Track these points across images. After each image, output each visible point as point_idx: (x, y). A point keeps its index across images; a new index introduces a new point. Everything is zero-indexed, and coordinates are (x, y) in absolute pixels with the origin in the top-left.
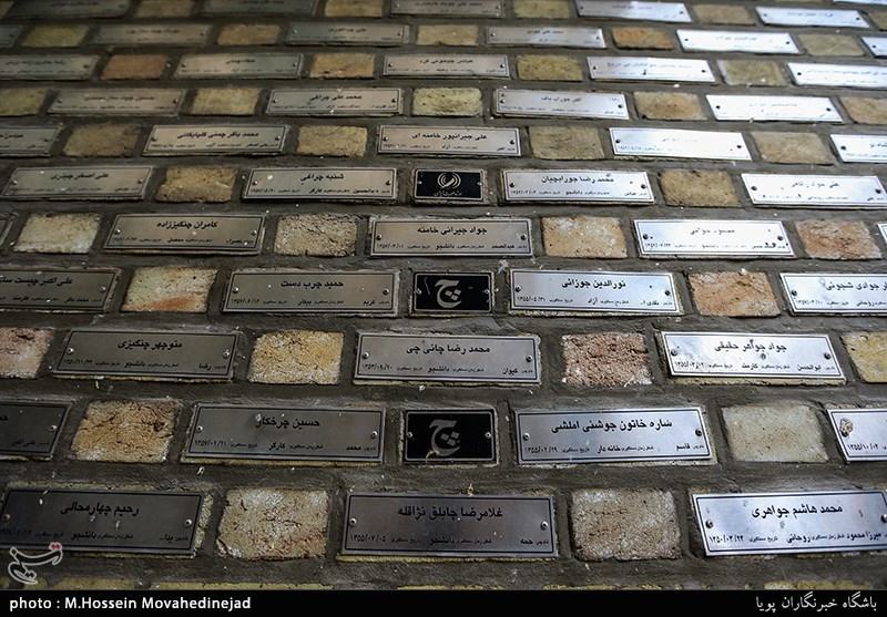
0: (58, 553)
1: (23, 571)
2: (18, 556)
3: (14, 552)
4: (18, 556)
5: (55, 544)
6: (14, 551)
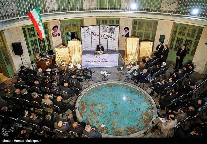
0: (13, 129)
1: (5, 133)
2: (4, 130)
3: (3, 129)
4: (4, 130)
5: (13, 127)
6: (3, 129)
